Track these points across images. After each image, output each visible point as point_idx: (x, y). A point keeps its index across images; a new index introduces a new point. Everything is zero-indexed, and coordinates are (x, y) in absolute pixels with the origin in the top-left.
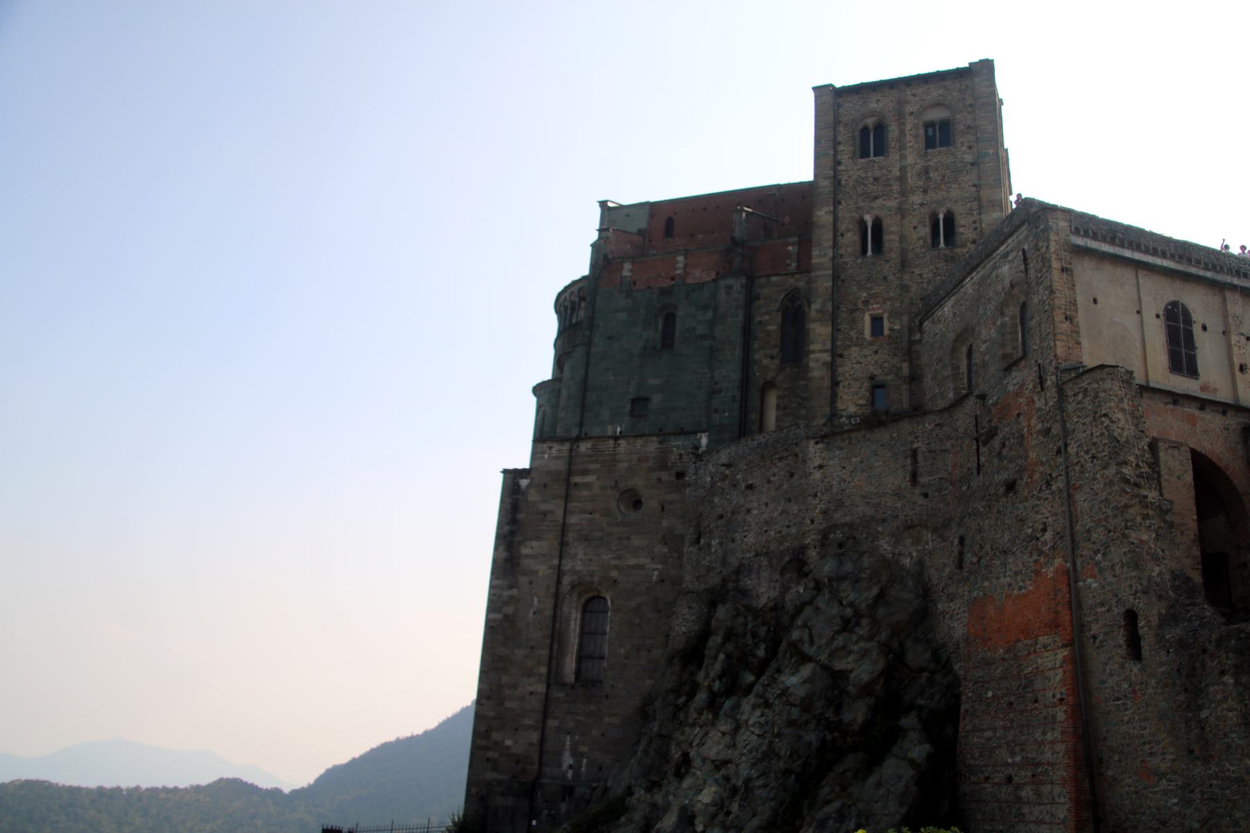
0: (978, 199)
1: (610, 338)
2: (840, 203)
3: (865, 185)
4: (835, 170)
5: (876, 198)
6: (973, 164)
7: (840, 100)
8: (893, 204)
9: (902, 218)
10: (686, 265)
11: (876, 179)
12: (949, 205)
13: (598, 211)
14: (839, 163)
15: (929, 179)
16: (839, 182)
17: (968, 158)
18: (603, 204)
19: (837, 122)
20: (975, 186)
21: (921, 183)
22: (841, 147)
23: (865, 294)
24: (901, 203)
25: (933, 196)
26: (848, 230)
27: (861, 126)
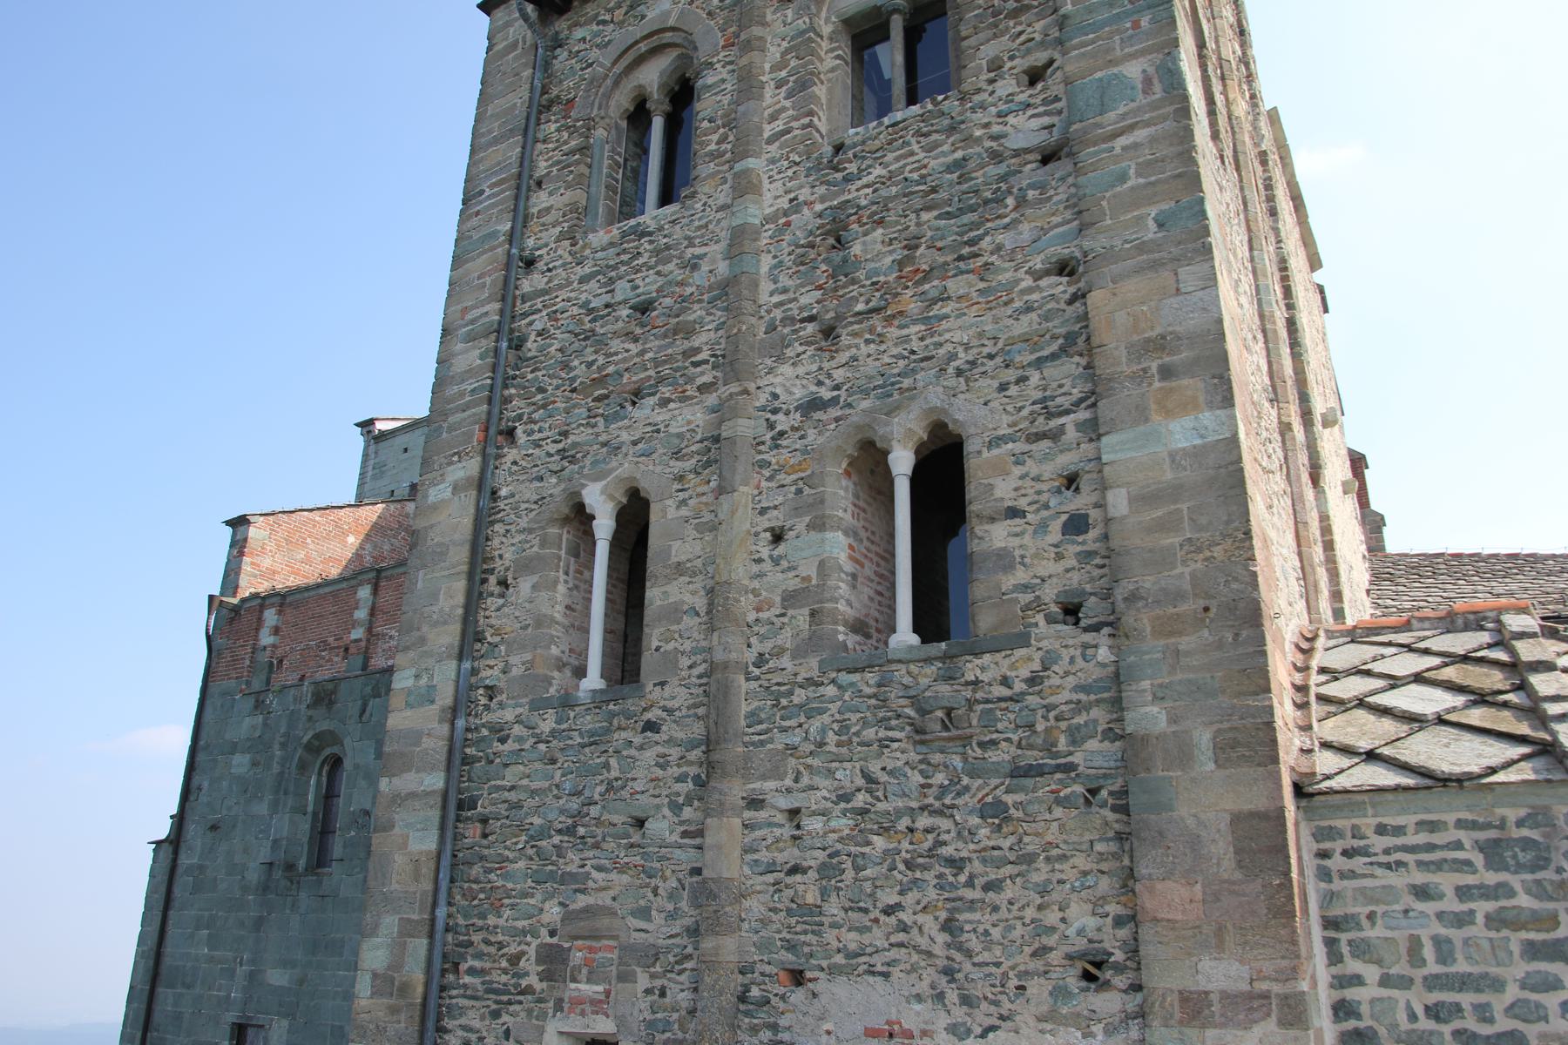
0: (1079, 340)
1: (214, 828)
2: (510, 433)
3: (600, 344)
4: (506, 294)
5: (637, 395)
6: (1048, 157)
7: (561, 25)
8: (691, 417)
9: (721, 491)
10: (373, 612)
11: (644, 308)
12: (935, 397)
13: (358, 441)
14: (530, 263)
15: (844, 270)
16: (518, 344)
17: (1026, 130)
18: (366, 425)
19: (542, 105)
20: (1064, 268)
21: (809, 298)
22: (541, 200)
23: (553, 912)
24: (722, 412)
25: (863, 354)
26: (525, 566)
27: (622, 101)
